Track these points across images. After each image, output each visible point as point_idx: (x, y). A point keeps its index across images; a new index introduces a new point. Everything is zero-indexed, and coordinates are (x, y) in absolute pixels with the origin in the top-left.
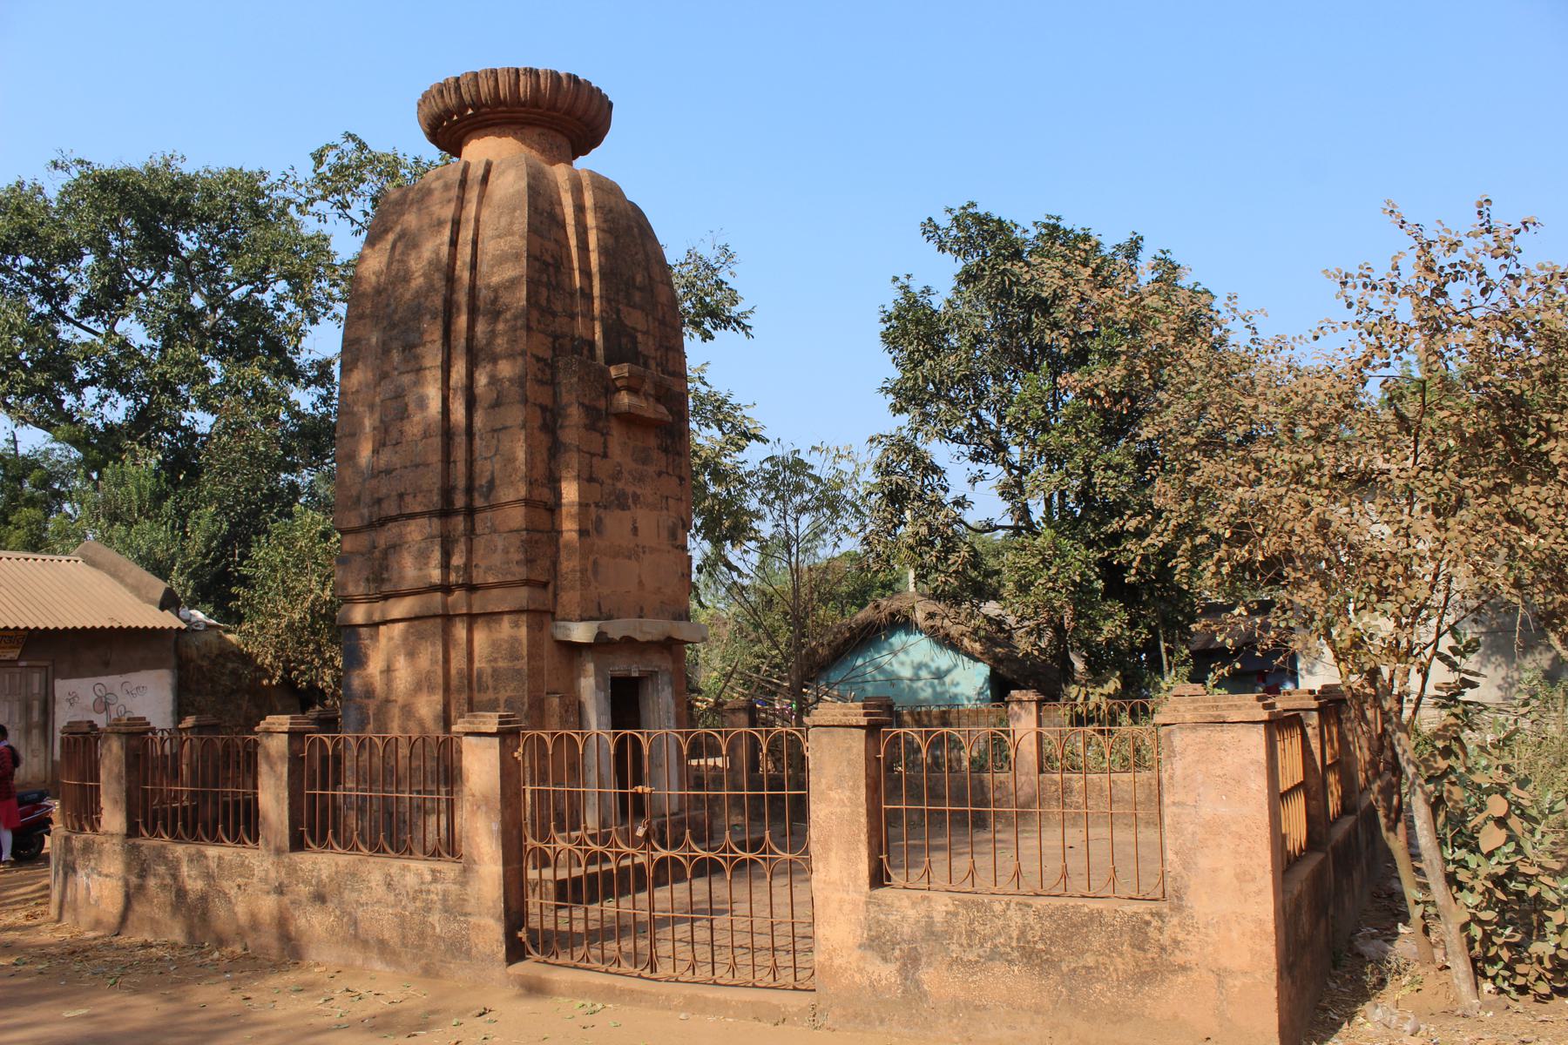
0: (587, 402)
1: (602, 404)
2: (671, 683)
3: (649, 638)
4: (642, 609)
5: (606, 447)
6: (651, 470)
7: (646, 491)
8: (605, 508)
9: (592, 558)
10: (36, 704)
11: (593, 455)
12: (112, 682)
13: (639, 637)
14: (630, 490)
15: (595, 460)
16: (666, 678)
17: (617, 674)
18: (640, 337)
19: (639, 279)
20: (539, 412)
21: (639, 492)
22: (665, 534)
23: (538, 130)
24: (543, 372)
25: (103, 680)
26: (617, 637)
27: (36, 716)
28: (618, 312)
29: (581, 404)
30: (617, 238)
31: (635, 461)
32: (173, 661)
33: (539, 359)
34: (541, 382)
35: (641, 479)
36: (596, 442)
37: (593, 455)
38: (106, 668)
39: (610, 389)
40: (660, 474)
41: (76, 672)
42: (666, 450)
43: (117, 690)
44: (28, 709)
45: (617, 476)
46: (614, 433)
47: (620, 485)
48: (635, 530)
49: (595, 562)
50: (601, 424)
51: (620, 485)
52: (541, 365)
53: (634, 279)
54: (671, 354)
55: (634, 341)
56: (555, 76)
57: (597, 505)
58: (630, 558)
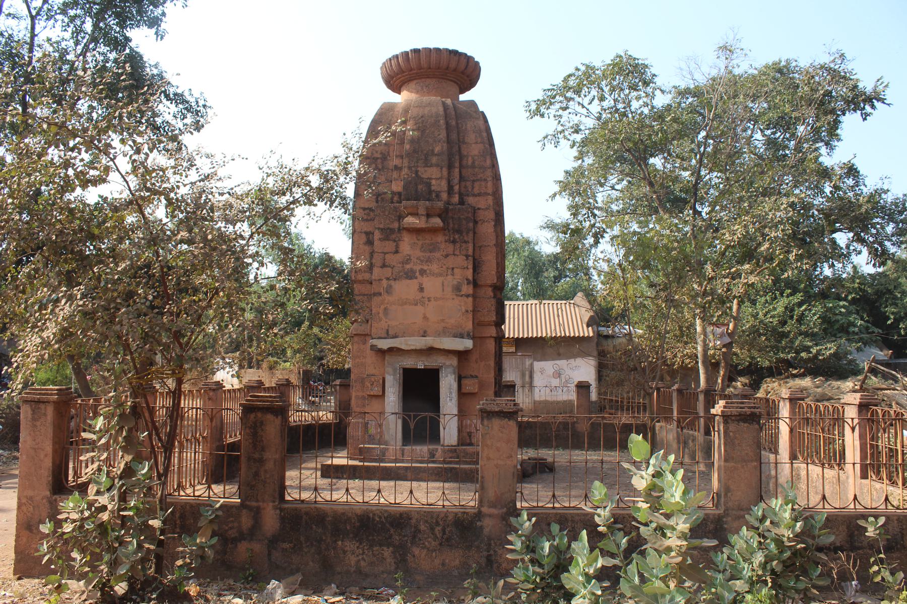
0: (382, 226)
1: (396, 225)
2: (454, 373)
3: (413, 348)
4: (425, 332)
5: (397, 247)
6: (437, 255)
7: (435, 267)
8: (395, 280)
9: (383, 307)
10: (527, 373)
11: (385, 253)
12: (562, 363)
13: (403, 347)
14: (417, 268)
15: (387, 256)
16: (450, 370)
17: (407, 366)
18: (433, 182)
19: (437, 149)
20: (364, 236)
21: (425, 268)
22: (449, 289)
23: (415, 82)
24: (368, 215)
25: (557, 362)
26: (385, 347)
27: (527, 378)
28: (417, 172)
29: (379, 229)
30: (423, 132)
31: (424, 251)
32: (595, 353)
33: (364, 209)
34: (367, 220)
35: (429, 261)
36: (390, 246)
37: (385, 253)
38: (559, 356)
39: (400, 218)
40: (447, 256)
41: (544, 358)
42: (454, 242)
43: (565, 367)
44: (523, 375)
45: (408, 260)
46: (406, 239)
47: (408, 267)
48: (421, 289)
49: (386, 309)
50: (393, 236)
51: (408, 267)
52: (366, 212)
53: (433, 151)
54: (477, 185)
55: (429, 185)
56: (406, 54)
57: (388, 279)
58: (416, 305)
